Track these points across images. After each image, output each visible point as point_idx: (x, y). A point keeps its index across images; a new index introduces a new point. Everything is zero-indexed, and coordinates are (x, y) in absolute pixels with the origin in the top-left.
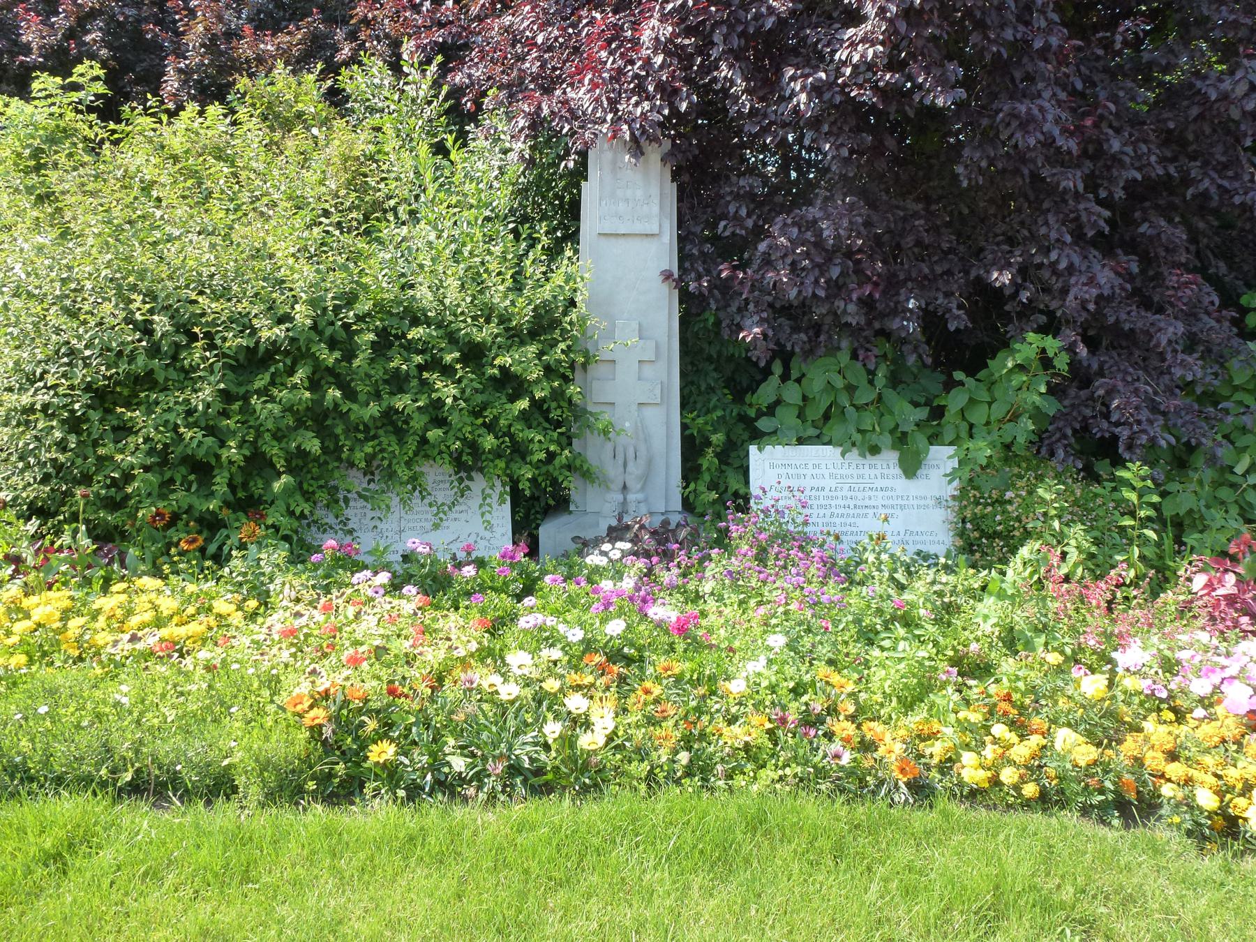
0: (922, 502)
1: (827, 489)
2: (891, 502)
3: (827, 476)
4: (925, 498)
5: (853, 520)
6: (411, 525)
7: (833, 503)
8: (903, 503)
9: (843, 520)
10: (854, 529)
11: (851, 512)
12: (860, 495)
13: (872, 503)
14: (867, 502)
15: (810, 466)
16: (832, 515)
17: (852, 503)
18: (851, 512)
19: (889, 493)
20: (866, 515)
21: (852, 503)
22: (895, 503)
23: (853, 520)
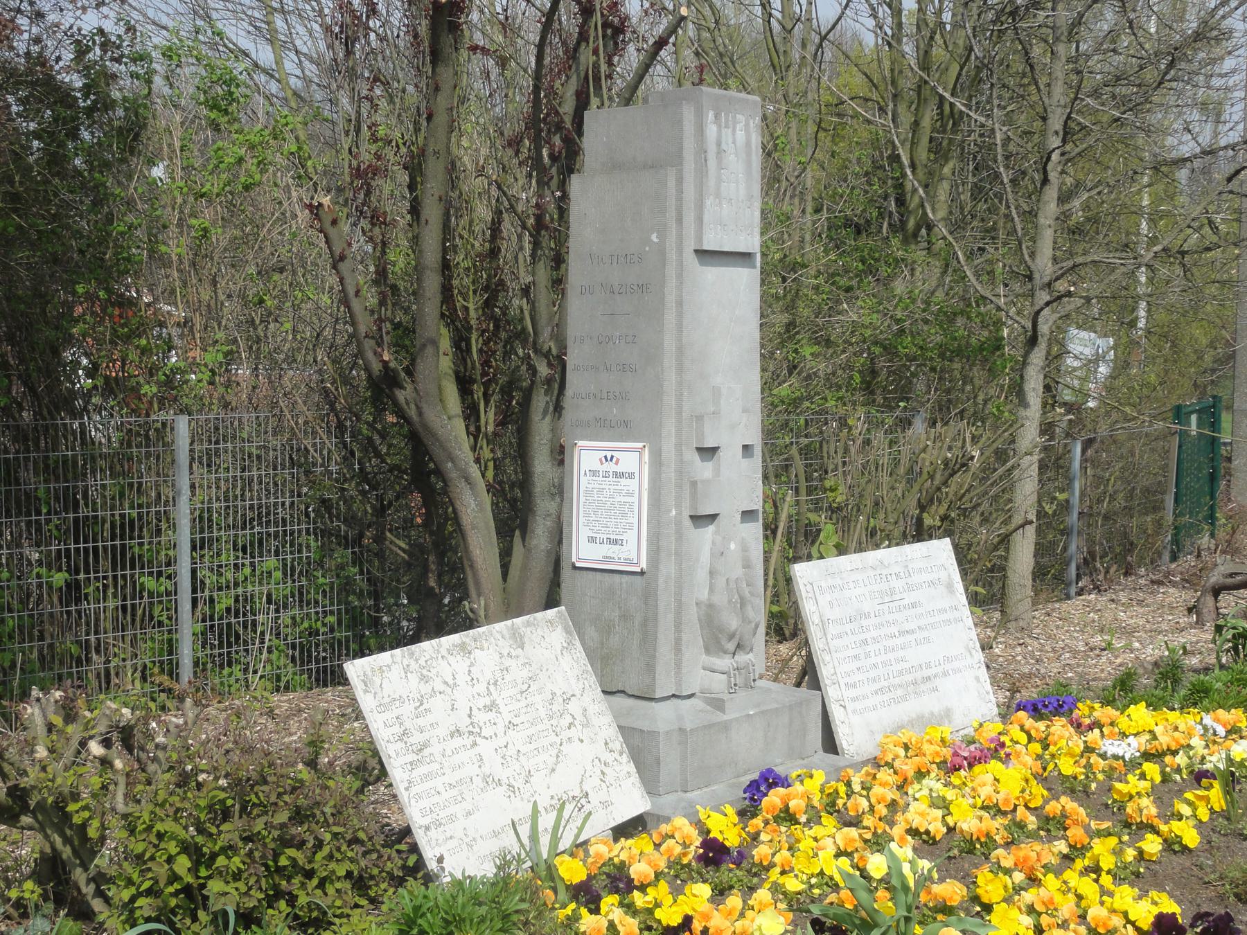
4: (945, 611)
10: (907, 665)
14: (907, 627)
18: (898, 641)
19: (920, 610)
23: (901, 653)
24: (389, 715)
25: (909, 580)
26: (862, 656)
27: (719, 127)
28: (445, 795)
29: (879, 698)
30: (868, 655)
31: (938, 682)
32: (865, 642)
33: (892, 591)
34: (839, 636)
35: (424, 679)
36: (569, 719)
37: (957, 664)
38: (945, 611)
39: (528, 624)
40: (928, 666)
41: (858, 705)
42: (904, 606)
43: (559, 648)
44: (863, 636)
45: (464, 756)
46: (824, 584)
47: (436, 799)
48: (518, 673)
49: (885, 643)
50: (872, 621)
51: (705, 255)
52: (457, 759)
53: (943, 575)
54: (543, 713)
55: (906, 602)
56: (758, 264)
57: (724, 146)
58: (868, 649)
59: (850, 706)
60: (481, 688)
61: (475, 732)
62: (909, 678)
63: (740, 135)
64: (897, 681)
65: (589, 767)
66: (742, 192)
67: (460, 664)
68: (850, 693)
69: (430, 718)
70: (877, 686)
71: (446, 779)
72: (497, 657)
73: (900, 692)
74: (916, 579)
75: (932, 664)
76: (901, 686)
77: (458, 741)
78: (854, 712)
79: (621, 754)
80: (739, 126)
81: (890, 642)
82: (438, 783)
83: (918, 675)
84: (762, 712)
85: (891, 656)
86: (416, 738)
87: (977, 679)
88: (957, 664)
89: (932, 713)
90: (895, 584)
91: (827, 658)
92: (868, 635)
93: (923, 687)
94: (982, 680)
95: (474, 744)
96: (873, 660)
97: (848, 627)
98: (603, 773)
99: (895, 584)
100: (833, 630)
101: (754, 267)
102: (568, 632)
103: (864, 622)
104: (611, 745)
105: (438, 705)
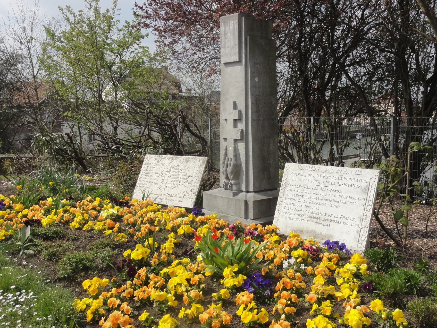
0: (354, 201)
1: (311, 188)
2: (337, 199)
3: (313, 181)
4: (355, 199)
5: (317, 206)
6: (169, 185)
7: (312, 196)
8: (343, 200)
9: (314, 205)
11: (319, 201)
12: (324, 193)
13: (330, 198)
14: (327, 197)
15: (307, 175)
16: (310, 202)
17: (320, 197)
18: (319, 201)
19: (338, 194)
20: (325, 205)
21: (320, 197)
22: (340, 199)
23: (317, 206)
24: (146, 166)
25: (340, 181)
26: (297, 201)
27: (225, 27)
28: (145, 183)
29: (297, 217)
30: (300, 201)
31: (331, 224)
32: (302, 196)
33: (327, 183)
34: (291, 190)
35: (158, 162)
36: (186, 180)
37: (347, 221)
38: (355, 199)
39: (193, 158)
40: (330, 215)
41: (286, 215)
42: (331, 190)
43: (197, 165)
44: (302, 194)
45: (155, 178)
46: (294, 172)
47: (143, 183)
48: (181, 167)
49: (311, 199)
50: (310, 190)
51: (226, 64)
52: (153, 178)
53: (364, 185)
54: (180, 177)
55: (333, 189)
56: (244, 64)
57: (226, 32)
58: (301, 199)
59: (282, 214)
60: (169, 167)
61: (161, 175)
62: (317, 216)
63: (231, 27)
64: (309, 215)
65: (182, 192)
66: (232, 43)
67: (168, 161)
68: (285, 210)
69: (154, 169)
70: (298, 212)
71: (148, 180)
72: (178, 163)
73: (308, 219)
74: (344, 182)
75: (333, 216)
76: (311, 217)
77: (156, 175)
78: (282, 216)
79: (194, 193)
80: (231, 24)
81: (315, 200)
82: (145, 180)
83: (322, 217)
84: (226, 197)
85: (312, 205)
86: (148, 171)
87: (359, 232)
88: (347, 221)
89: (321, 233)
90: (331, 180)
91: (282, 196)
92: (305, 195)
93: (322, 222)
94: (361, 234)
95: (159, 177)
96: (302, 203)
97: (296, 189)
98: (185, 195)
99: (331, 180)
100: (289, 188)
101: (242, 65)
102: (203, 163)
103: (305, 190)
104: (193, 190)
105: (157, 167)
